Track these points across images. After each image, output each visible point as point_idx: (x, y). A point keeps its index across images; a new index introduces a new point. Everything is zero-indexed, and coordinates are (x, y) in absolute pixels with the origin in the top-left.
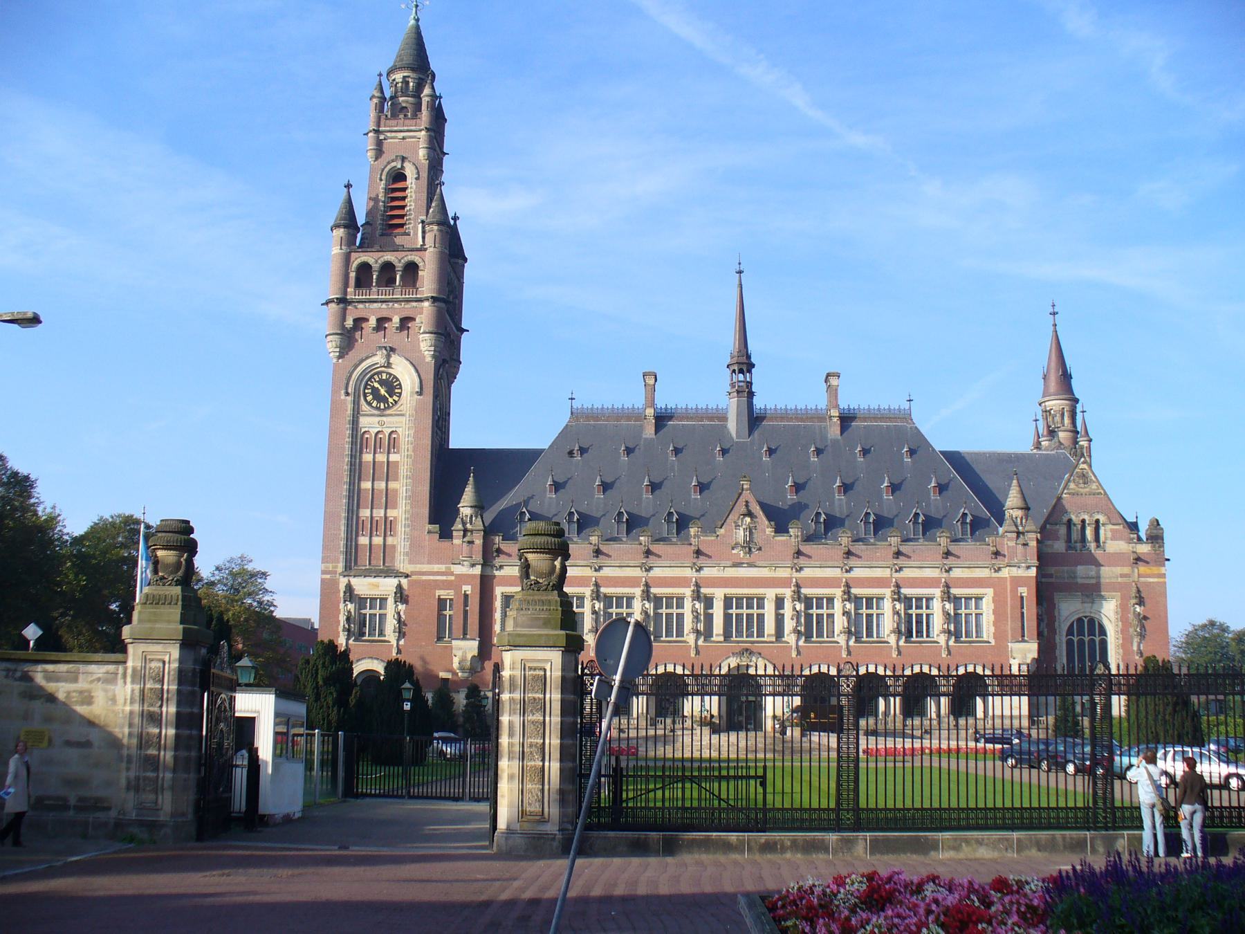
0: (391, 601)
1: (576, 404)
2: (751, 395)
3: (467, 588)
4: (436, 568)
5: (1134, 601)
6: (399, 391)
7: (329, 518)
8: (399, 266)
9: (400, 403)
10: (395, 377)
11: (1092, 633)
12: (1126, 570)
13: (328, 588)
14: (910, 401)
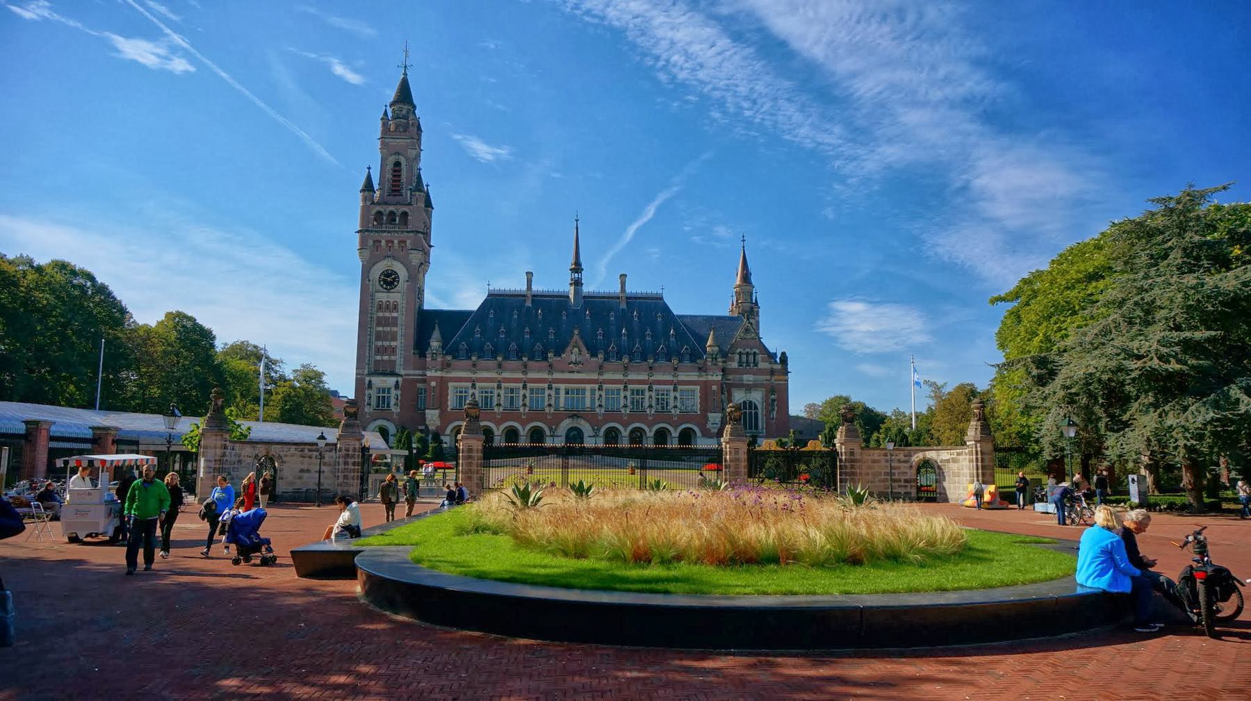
0: (393, 389)
3: (433, 384)
4: (417, 372)
8: (399, 213)
11: (750, 408)
12: (768, 377)
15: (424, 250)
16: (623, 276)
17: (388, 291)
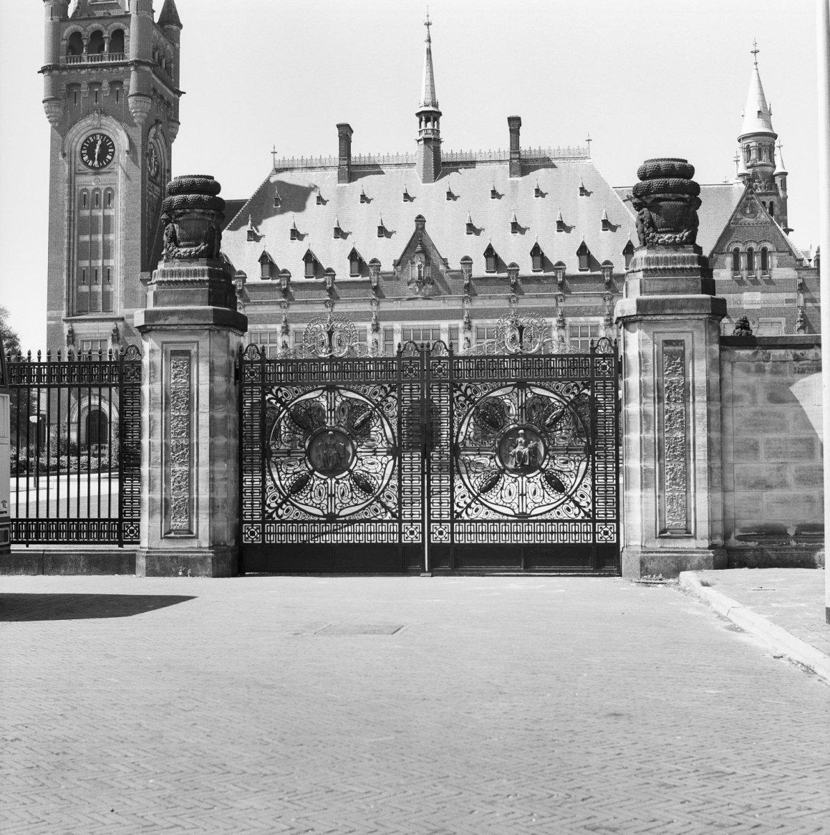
0: (110, 341)
1: (279, 157)
2: (438, 141)
5: (799, 325)
6: (112, 150)
7: (52, 267)
9: (112, 163)
10: (108, 138)
12: (792, 296)
13: (53, 333)
14: (589, 140)
15: (155, 90)
16: (515, 123)
17: (97, 171)
